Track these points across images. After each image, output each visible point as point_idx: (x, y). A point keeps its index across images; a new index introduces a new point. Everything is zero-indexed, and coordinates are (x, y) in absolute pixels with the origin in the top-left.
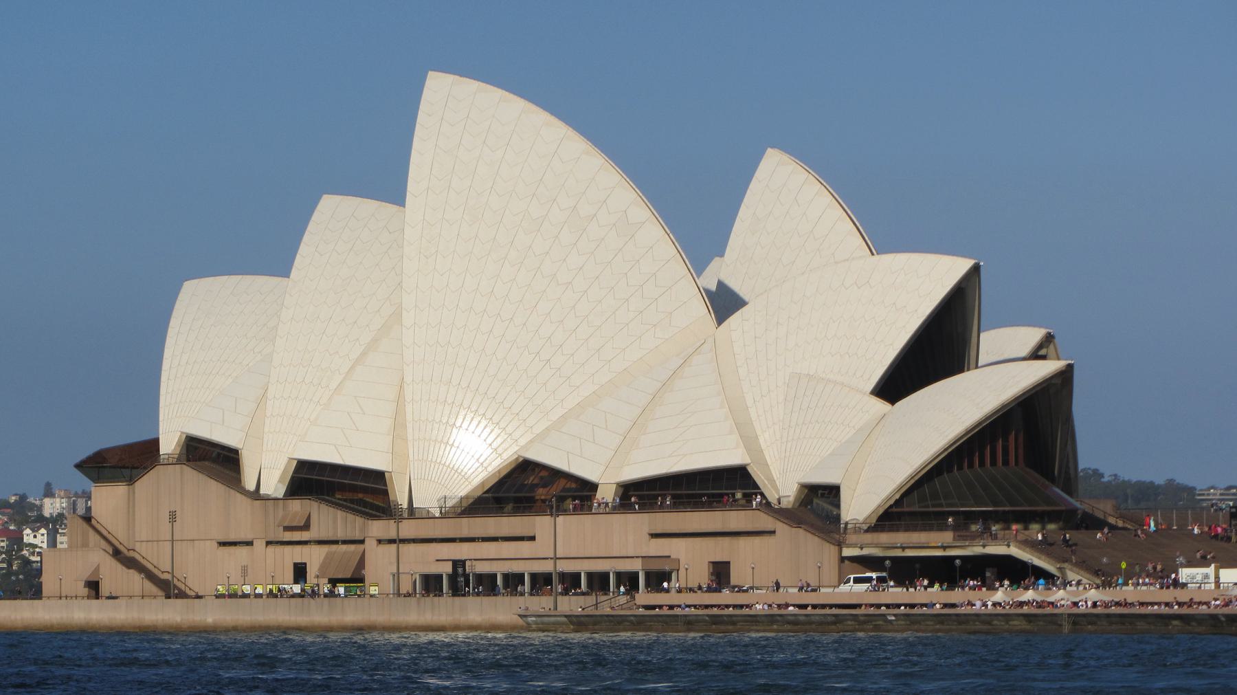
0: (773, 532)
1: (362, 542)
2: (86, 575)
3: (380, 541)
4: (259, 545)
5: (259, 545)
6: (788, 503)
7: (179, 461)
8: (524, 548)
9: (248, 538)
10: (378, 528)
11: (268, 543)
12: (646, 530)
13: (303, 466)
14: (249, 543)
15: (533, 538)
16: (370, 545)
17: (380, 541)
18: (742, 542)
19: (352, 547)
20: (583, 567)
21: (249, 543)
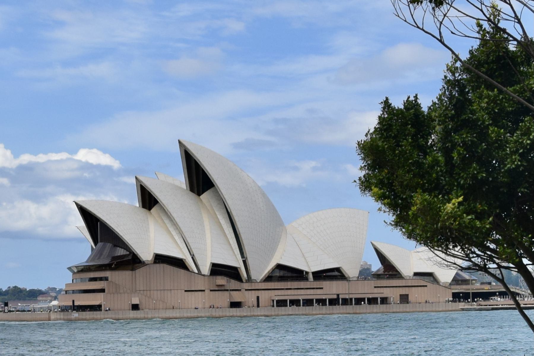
0: (426, 286)
1: (240, 290)
2: (136, 301)
3: (246, 290)
4: (207, 291)
5: (207, 291)
6: (408, 278)
7: (155, 262)
8: (319, 291)
10: (246, 286)
11: (211, 291)
12: (373, 286)
13: (214, 265)
14: (204, 291)
15: (322, 288)
16: (243, 291)
17: (246, 290)
18: (413, 288)
19: (237, 292)
20: (366, 296)
21: (204, 291)
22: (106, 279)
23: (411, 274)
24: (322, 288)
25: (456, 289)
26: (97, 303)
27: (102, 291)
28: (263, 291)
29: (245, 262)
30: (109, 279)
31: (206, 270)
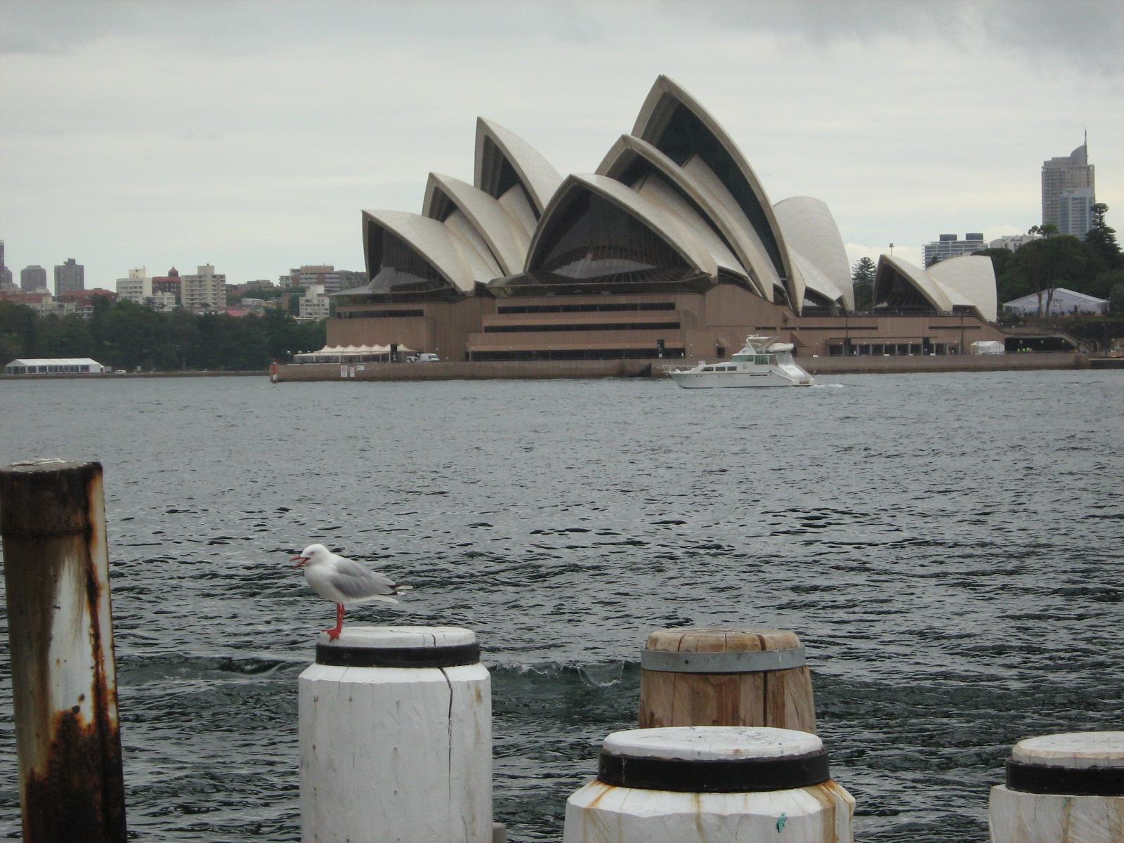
0: (979, 328)
3: (801, 329)
4: (778, 329)
5: (778, 329)
8: (874, 333)
9: (774, 326)
11: (782, 329)
15: (876, 328)
17: (801, 329)
22: (671, 307)
23: (950, 309)
24: (876, 328)
25: (1007, 333)
26: (679, 345)
27: (676, 326)
28: (818, 332)
29: (785, 283)
30: (678, 306)
31: (770, 295)
